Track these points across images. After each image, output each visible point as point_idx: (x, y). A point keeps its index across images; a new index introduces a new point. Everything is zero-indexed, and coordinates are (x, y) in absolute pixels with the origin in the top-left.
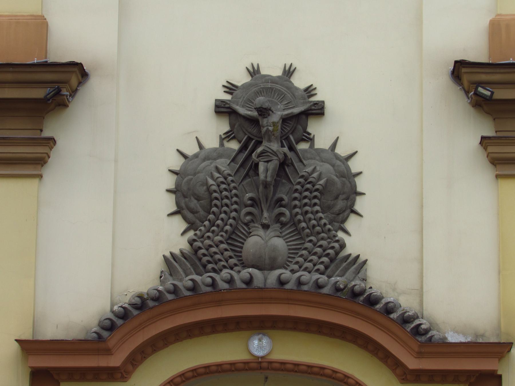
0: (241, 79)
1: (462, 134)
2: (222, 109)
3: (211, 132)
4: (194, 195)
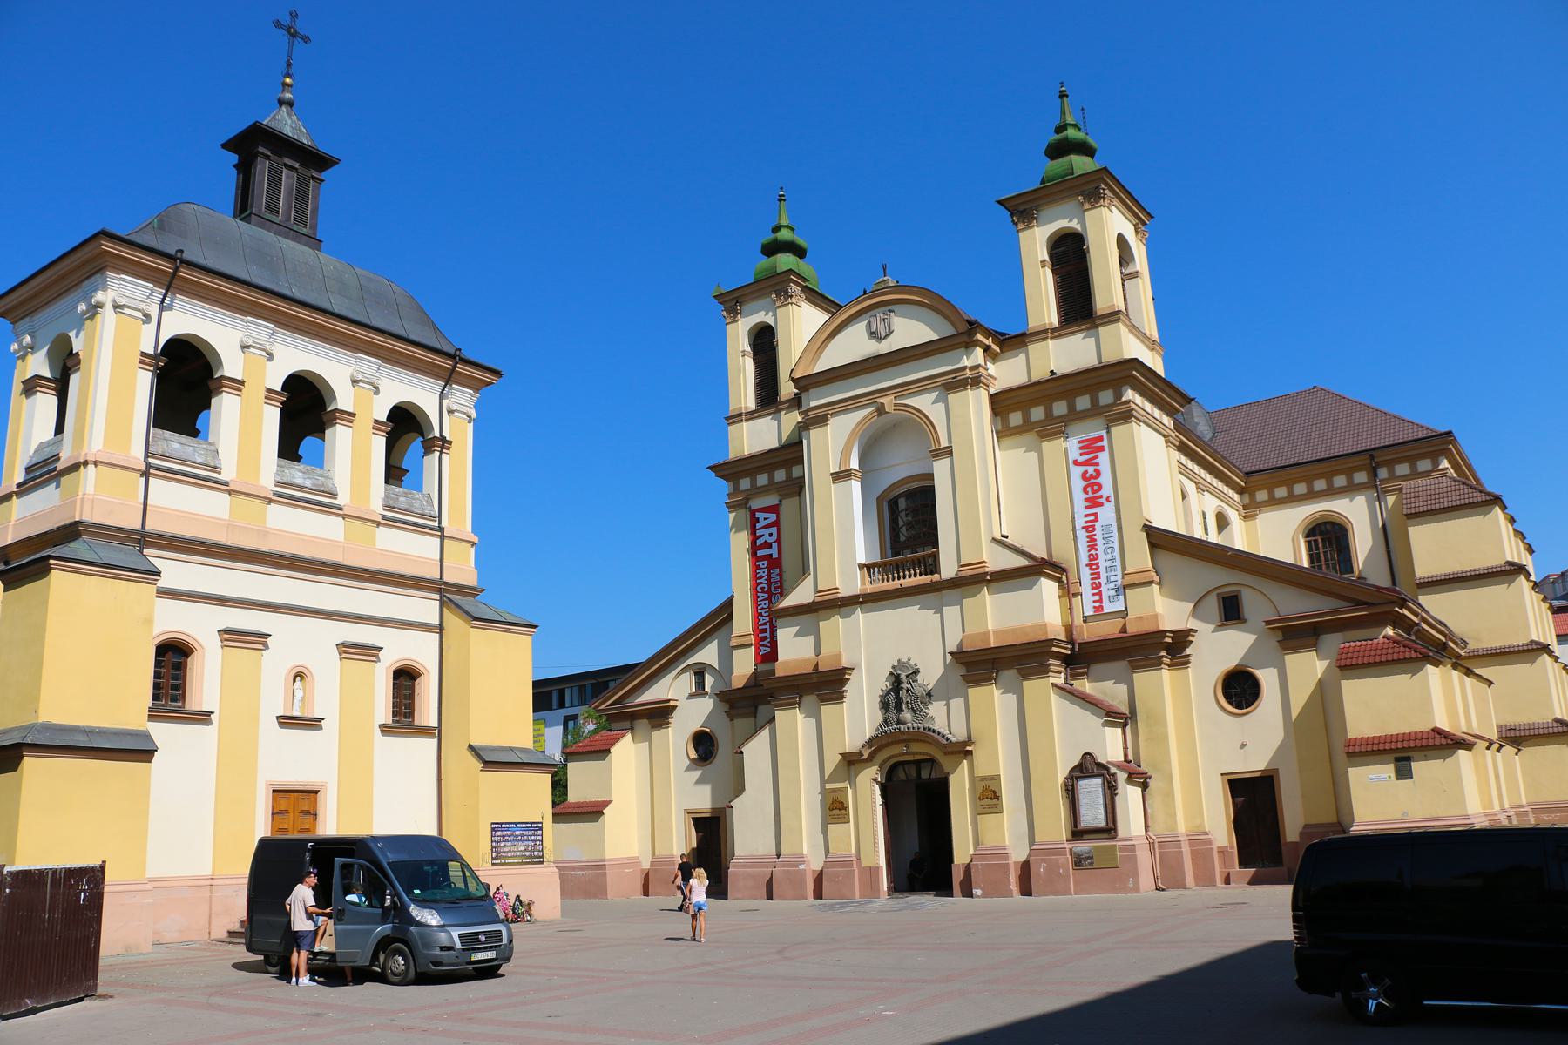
4: (885, 705)
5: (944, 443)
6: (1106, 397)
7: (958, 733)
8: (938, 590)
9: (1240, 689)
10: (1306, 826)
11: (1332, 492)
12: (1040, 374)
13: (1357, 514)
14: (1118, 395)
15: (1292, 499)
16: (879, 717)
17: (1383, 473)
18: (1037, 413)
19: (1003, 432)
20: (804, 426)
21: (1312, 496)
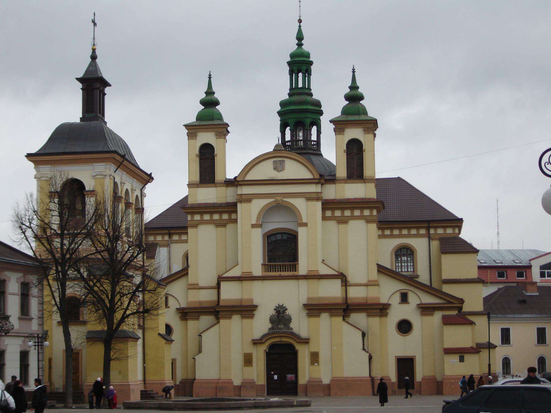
0: (277, 305)
1: (304, 313)
2: (275, 309)
3: (274, 312)
4: (272, 320)
5: (304, 221)
6: (367, 213)
7: (304, 334)
8: (298, 279)
9: (404, 327)
10: (424, 376)
11: (409, 236)
12: (339, 197)
13: (420, 245)
14: (371, 212)
15: (392, 236)
16: (270, 326)
17: (432, 231)
18: (338, 213)
19: (324, 218)
20: (241, 202)
21: (401, 236)
